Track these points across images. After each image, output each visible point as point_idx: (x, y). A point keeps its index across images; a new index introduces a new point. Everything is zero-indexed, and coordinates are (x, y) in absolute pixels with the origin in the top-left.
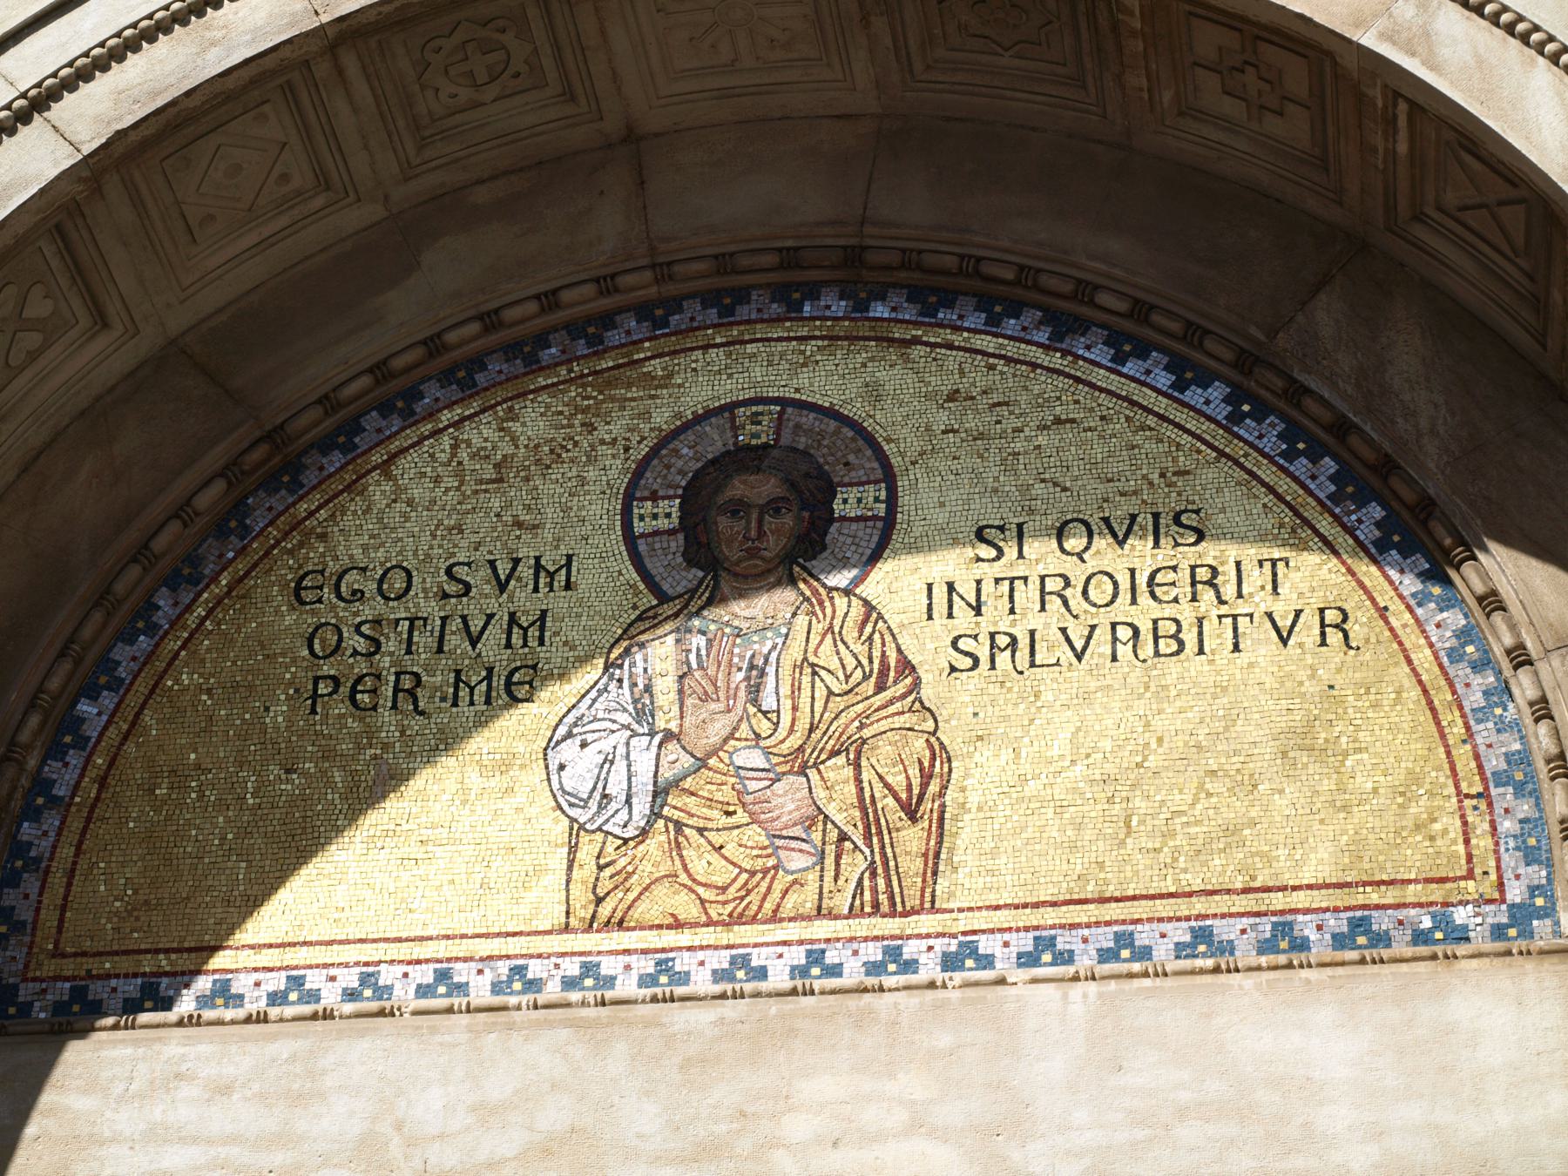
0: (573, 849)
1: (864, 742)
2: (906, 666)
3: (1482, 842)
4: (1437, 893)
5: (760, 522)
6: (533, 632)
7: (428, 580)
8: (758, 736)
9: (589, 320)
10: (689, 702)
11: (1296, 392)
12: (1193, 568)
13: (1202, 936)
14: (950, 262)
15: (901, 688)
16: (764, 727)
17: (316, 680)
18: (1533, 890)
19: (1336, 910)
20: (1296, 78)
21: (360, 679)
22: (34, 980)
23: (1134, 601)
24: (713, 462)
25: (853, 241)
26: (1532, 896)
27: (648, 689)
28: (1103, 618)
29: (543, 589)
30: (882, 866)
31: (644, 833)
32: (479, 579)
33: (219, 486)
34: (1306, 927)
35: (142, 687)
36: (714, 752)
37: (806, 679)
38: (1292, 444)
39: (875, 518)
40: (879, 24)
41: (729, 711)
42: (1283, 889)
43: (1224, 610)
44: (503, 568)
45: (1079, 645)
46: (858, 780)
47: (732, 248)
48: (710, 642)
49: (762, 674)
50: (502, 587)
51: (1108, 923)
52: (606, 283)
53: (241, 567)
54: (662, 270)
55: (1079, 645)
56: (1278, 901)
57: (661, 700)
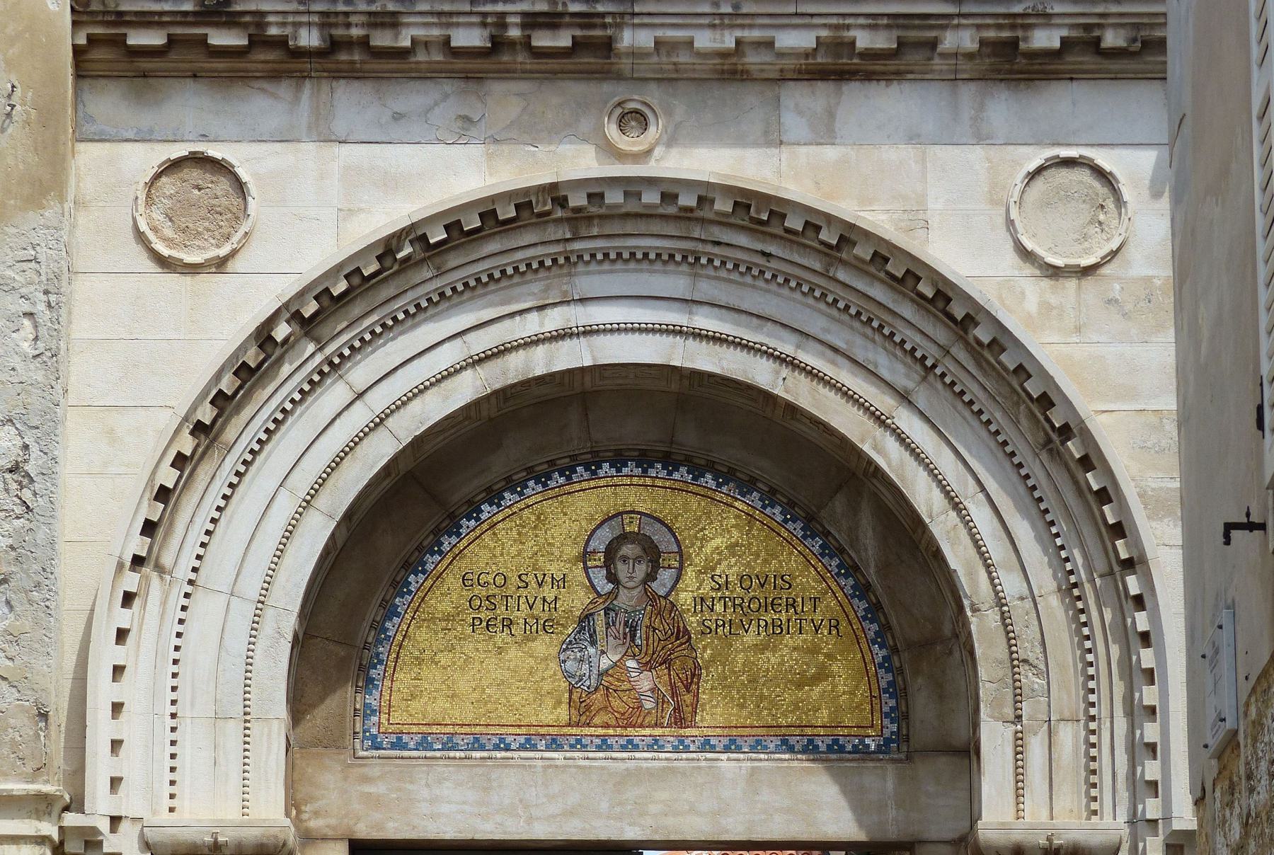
0: (571, 692)
1: (672, 660)
2: (687, 632)
3: (877, 715)
4: (862, 732)
5: (634, 565)
6: (552, 606)
7: (514, 579)
8: (635, 656)
10: (611, 639)
11: (827, 534)
12: (787, 599)
14: (703, 462)
15: (683, 640)
17: (474, 618)
18: (892, 733)
19: (829, 735)
21: (489, 620)
22: (382, 733)
23: (766, 611)
24: (617, 538)
25: (666, 449)
26: (891, 735)
27: (595, 631)
29: (555, 587)
31: (596, 689)
32: (530, 578)
33: (431, 537)
36: (619, 660)
37: (651, 633)
38: (824, 551)
39: (674, 568)
41: (624, 644)
42: (811, 727)
43: (797, 616)
45: (746, 627)
46: (670, 675)
47: (621, 447)
48: (616, 614)
49: (636, 630)
50: (540, 585)
51: (753, 736)
53: (440, 568)
54: (594, 453)
55: (746, 627)
56: (809, 731)
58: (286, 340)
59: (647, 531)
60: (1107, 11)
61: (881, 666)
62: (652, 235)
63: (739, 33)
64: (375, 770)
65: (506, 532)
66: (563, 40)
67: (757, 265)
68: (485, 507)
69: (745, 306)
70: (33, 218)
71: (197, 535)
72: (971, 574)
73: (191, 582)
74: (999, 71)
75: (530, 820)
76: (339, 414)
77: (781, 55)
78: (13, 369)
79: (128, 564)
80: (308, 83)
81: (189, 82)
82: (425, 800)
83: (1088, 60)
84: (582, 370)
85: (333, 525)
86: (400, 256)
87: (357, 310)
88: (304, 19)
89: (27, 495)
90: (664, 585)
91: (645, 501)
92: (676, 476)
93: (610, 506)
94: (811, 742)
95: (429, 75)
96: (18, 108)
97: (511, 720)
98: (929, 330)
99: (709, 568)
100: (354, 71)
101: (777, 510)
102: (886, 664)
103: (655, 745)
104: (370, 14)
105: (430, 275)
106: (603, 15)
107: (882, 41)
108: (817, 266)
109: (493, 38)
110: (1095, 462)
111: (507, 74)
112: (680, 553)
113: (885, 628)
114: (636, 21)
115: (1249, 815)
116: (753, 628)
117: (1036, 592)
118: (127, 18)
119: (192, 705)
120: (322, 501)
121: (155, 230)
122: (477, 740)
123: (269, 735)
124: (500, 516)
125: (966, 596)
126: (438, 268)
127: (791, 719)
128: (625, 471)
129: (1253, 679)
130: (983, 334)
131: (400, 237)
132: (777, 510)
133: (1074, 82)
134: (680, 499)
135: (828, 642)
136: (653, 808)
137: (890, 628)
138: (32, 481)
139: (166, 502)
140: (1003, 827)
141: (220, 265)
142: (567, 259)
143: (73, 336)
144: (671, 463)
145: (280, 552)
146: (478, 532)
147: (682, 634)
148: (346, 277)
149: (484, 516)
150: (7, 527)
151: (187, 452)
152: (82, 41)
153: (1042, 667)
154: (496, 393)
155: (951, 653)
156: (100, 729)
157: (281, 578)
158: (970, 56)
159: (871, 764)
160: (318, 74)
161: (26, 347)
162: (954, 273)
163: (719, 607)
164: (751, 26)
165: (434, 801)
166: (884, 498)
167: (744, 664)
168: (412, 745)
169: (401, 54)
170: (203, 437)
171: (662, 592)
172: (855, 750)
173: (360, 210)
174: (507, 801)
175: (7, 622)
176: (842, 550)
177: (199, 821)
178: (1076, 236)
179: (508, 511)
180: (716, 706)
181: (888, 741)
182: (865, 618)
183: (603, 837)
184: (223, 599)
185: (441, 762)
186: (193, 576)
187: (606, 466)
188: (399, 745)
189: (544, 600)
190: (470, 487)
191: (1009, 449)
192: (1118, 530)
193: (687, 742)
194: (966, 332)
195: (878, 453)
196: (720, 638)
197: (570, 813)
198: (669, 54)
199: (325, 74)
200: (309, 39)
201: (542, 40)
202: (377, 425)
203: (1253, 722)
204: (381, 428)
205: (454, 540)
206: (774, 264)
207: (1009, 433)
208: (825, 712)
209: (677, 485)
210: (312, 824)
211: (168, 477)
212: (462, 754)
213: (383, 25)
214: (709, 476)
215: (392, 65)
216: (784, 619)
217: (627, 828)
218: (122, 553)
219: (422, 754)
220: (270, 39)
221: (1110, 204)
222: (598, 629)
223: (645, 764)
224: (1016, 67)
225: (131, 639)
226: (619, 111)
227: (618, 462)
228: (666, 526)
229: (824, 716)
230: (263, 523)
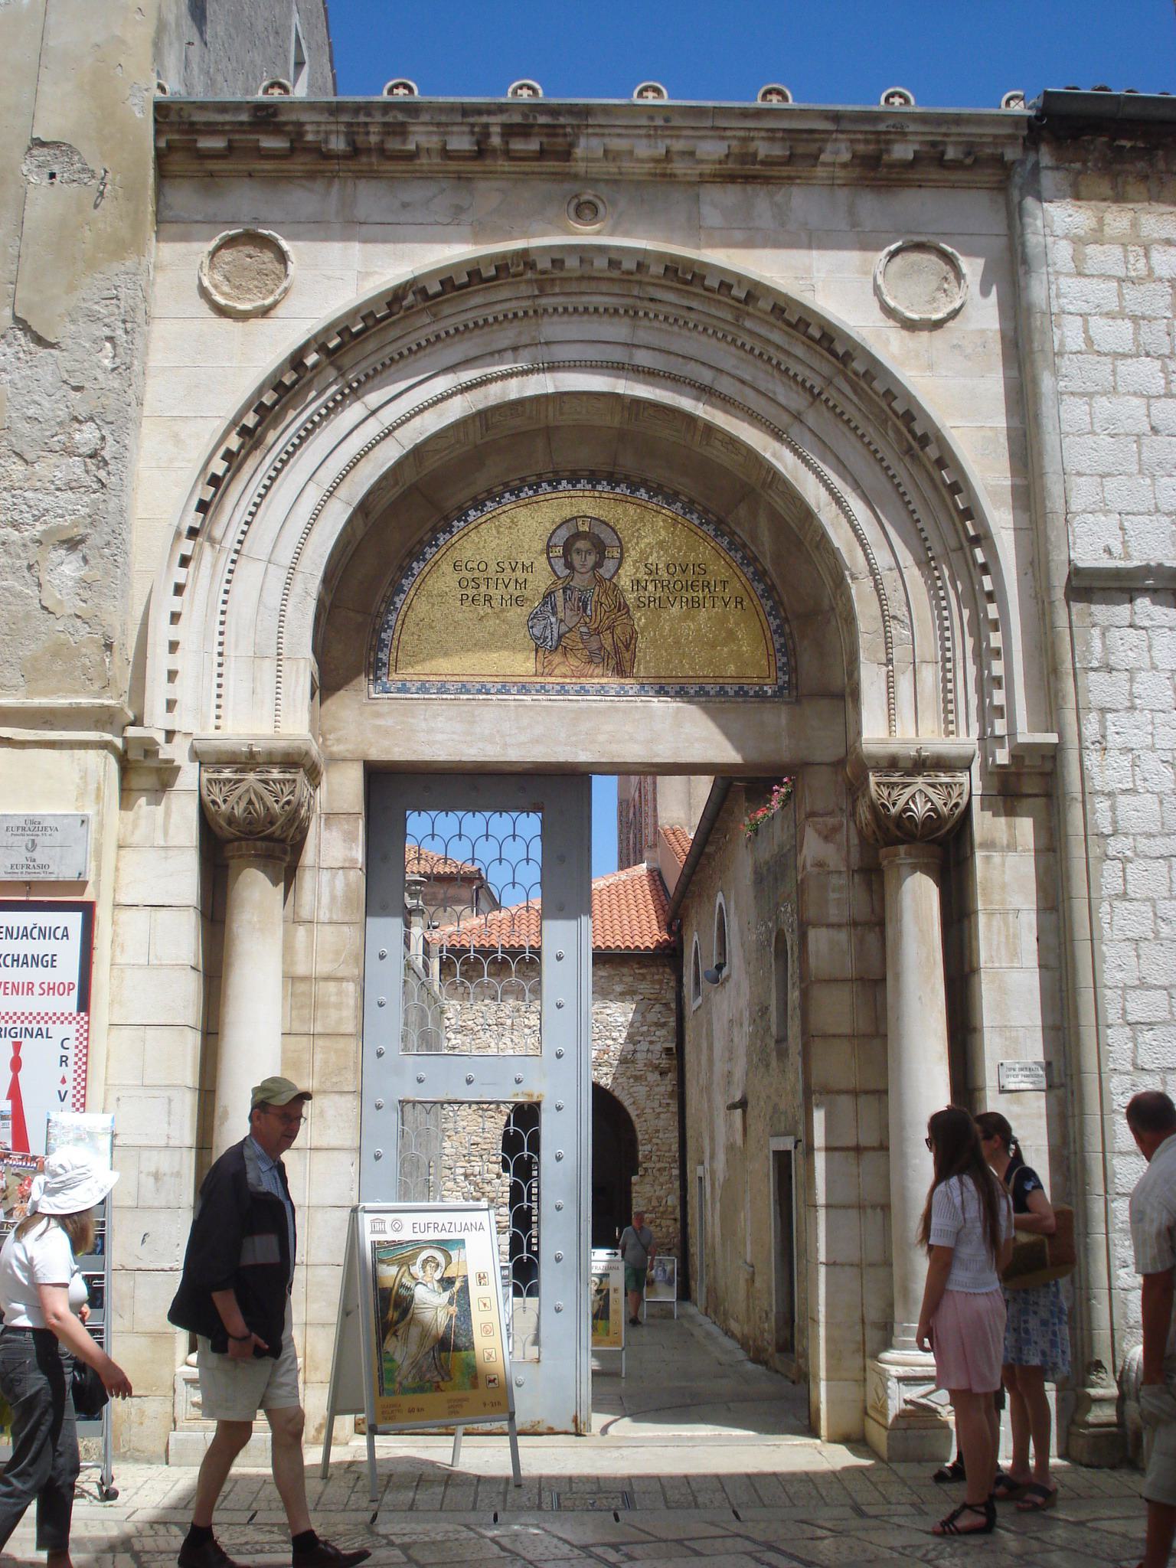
2: (626, 606)
3: (773, 669)
7: (493, 567)
9: (535, 484)
10: (568, 611)
14: (638, 480)
16: (588, 620)
18: (785, 682)
20: (744, 452)
28: (678, 594)
30: (619, 664)
31: (556, 648)
32: (506, 565)
34: (728, 688)
35: (412, 593)
40: (626, 413)
44: (513, 564)
50: (514, 570)
52: (539, 475)
53: (437, 557)
54: (555, 472)
56: (721, 681)
57: (559, 610)
58: (315, 366)
60: (949, 131)
61: (775, 632)
62: (602, 294)
63: (668, 142)
64: (384, 708)
66: (533, 145)
67: (682, 317)
68: (472, 512)
69: (674, 348)
70: (117, 267)
71: (242, 515)
72: (851, 551)
73: (237, 552)
74: (866, 179)
75: (505, 745)
76: (356, 427)
77: (701, 162)
78: (95, 379)
79: (185, 533)
80: (336, 180)
81: (247, 180)
82: (423, 731)
83: (935, 174)
84: (546, 396)
85: (350, 510)
86: (405, 303)
87: (371, 346)
88: (333, 128)
89: (102, 474)
90: (609, 571)
91: (594, 509)
92: (618, 490)
93: (567, 513)
95: (430, 175)
96: (109, 187)
97: (493, 671)
98: (816, 364)
99: (644, 557)
100: (371, 171)
101: (695, 516)
102: (779, 631)
103: (602, 691)
104: (385, 124)
105: (428, 321)
106: (563, 126)
107: (778, 151)
108: (730, 317)
109: (478, 143)
110: (948, 462)
111: (488, 174)
112: (621, 547)
113: (778, 605)
114: (590, 131)
117: (902, 565)
118: (198, 127)
119: (237, 646)
120: (342, 492)
121: (216, 287)
122: (464, 686)
123: (297, 671)
124: (483, 519)
125: (848, 569)
126: (435, 315)
128: (579, 486)
130: (859, 366)
131: (405, 288)
132: (695, 516)
133: (923, 190)
136: (601, 738)
137: (782, 604)
138: (106, 463)
139: (217, 488)
140: (882, 742)
141: (265, 312)
142: (535, 312)
143: (150, 364)
144: (613, 480)
145: (308, 531)
146: (466, 531)
147: (622, 607)
148: (364, 319)
149: (470, 519)
150: (86, 499)
151: (234, 448)
152: (162, 144)
153: (907, 621)
155: (829, 622)
156: (159, 661)
157: (309, 550)
158: (844, 165)
159: (768, 705)
160: (345, 174)
161: (107, 363)
162: (837, 318)
163: (651, 587)
164: (678, 137)
165: (431, 731)
166: (775, 505)
167: (670, 631)
168: (414, 689)
169: (411, 156)
170: (247, 438)
171: (607, 576)
172: (756, 695)
173: (376, 272)
174: (487, 732)
175: (82, 573)
176: (744, 546)
177: (239, 735)
178: (926, 299)
179: (489, 516)
180: (649, 662)
181: (781, 688)
182: (763, 596)
183: (562, 759)
184: (263, 565)
185: (436, 702)
186: (238, 547)
187: (564, 482)
188: (403, 689)
189: (517, 581)
191: (879, 456)
192: (968, 514)
193: (627, 688)
194: (845, 365)
195: (777, 459)
196: (652, 611)
197: (537, 741)
198: (614, 160)
199: (350, 174)
200: (338, 144)
201: (518, 145)
202: (387, 435)
204: (389, 438)
206: (693, 315)
207: (879, 444)
209: (618, 497)
210: (335, 749)
211: (219, 467)
212: (453, 697)
213: (395, 133)
214: (643, 490)
215: (402, 166)
216: (701, 596)
217: (580, 752)
218: (180, 524)
219: (422, 696)
220: (308, 145)
221: (951, 276)
222: (558, 604)
223: (594, 704)
224: (878, 176)
225: (186, 592)
226: (575, 201)
227: (573, 480)
228: (610, 527)
229: (731, 669)
230: (295, 508)
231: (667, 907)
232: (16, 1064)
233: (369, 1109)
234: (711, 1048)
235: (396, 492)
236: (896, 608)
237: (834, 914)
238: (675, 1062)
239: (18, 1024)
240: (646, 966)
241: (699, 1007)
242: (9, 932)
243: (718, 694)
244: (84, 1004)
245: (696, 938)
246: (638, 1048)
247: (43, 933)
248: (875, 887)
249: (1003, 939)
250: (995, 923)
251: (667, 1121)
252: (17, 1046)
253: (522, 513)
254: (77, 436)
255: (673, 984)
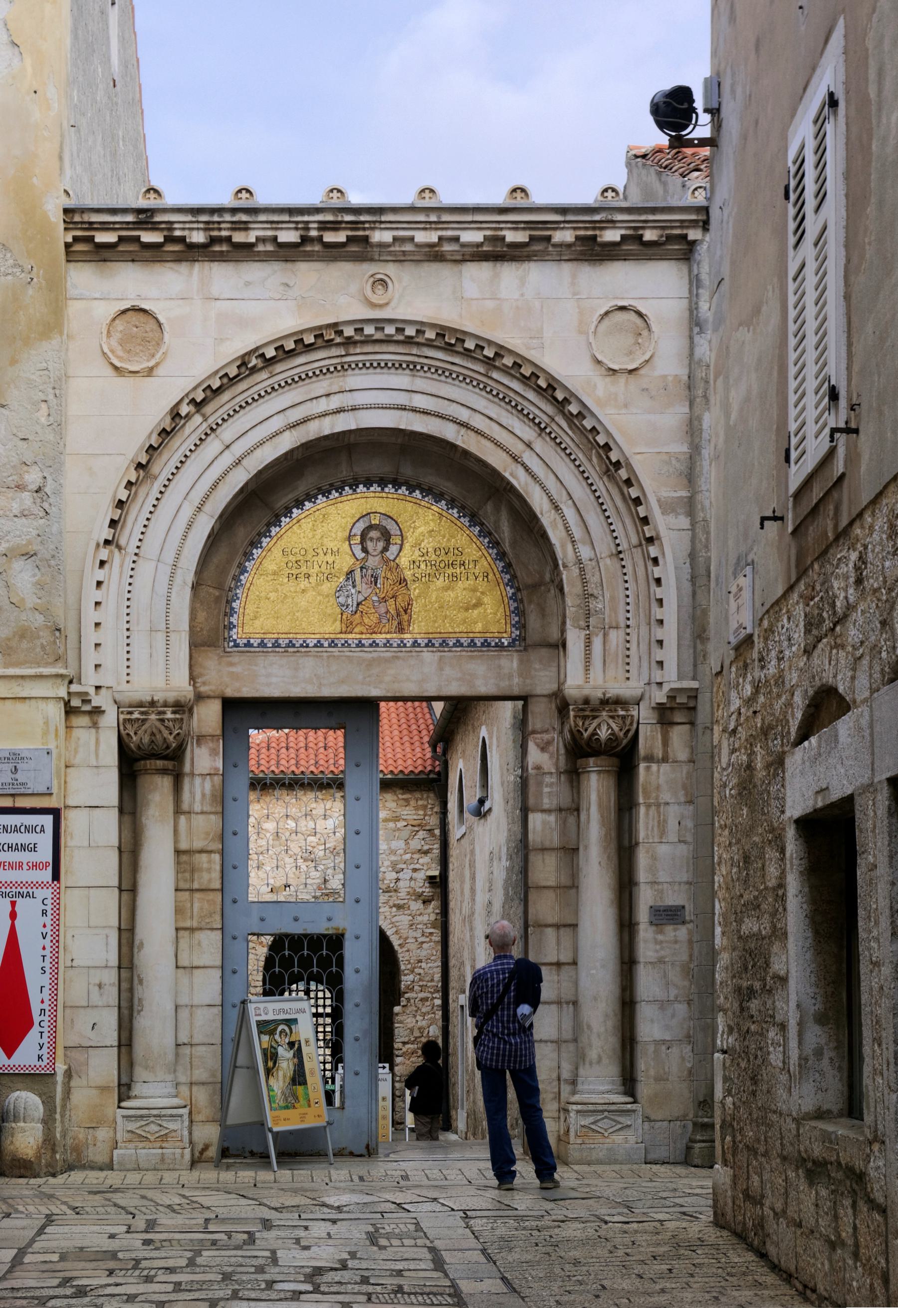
2: (405, 580)
3: (508, 626)
13: (458, 641)
32: (320, 551)
34: (476, 641)
54: (355, 479)
56: (471, 635)
59: (384, 523)
65: (307, 524)
68: (295, 510)
84: (350, 431)
86: (250, 366)
87: (226, 396)
92: (400, 491)
94: (472, 641)
99: (417, 544)
101: (455, 511)
102: (514, 598)
112: (402, 535)
113: (514, 577)
115: (759, 681)
116: (442, 579)
127: (462, 628)
128: (372, 489)
129: (767, 606)
132: (455, 511)
134: (402, 504)
135: (482, 585)
140: (579, 687)
144: (397, 484)
147: (403, 581)
149: (294, 516)
154: (302, 445)
163: (423, 566)
171: (392, 558)
172: (496, 645)
176: (490, 534)
181: (514, 640)
187: (361, 486)
190: (288, 498)
203: (766, 630)
205: (278, 529)
208: (480, 625)
214: (418, 492)
227: (368, 483)
229: (479, 627)
231: (431, 727)
232: (13, 915)
233: (228, 940)
234: (473, 878)
235: (240, 498)
236: (592, 589)
237: (546, 803)
238: (439, 890)
239: (14, 889)
240: (410, 791)
241: (463, 836)
242: (5, 829)
243: (469, 646)
244: (56, 876)
245: (461, 765)
246: (401, 875)
247: (28, 829)
248: (575, 784)
249: (656, 824)
250: (651, 813)
251: (432, 950)
252: (13, 904)
253: (332, 510)
254: (26, 477)
255: (437, 809)
